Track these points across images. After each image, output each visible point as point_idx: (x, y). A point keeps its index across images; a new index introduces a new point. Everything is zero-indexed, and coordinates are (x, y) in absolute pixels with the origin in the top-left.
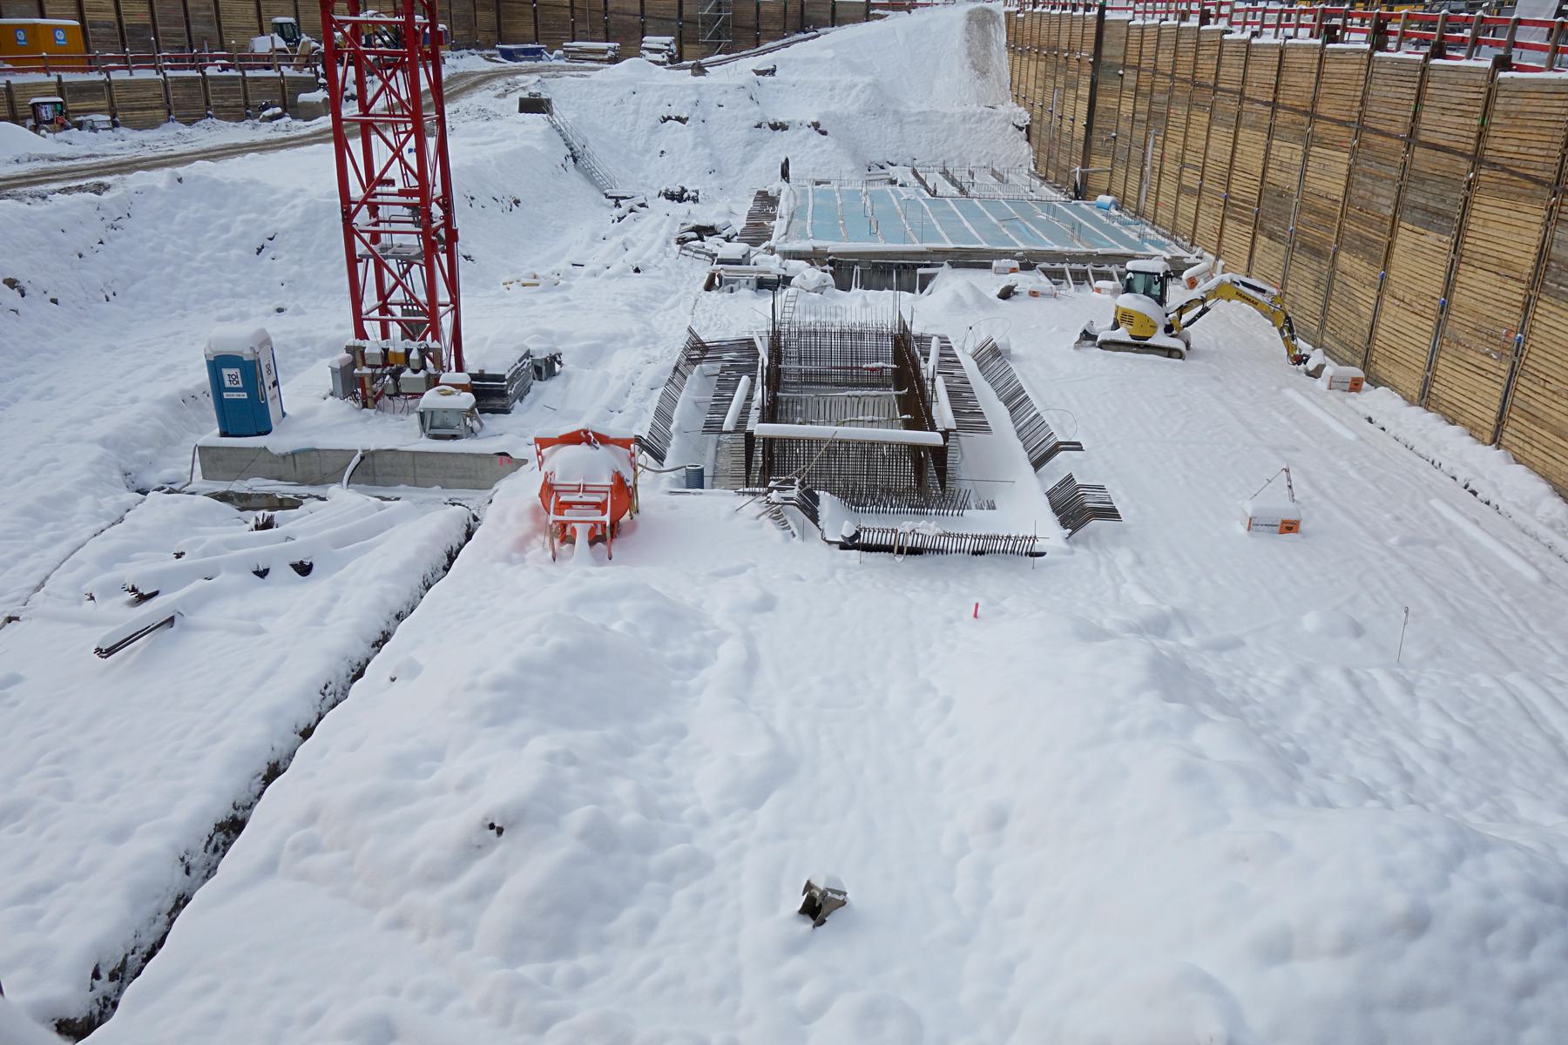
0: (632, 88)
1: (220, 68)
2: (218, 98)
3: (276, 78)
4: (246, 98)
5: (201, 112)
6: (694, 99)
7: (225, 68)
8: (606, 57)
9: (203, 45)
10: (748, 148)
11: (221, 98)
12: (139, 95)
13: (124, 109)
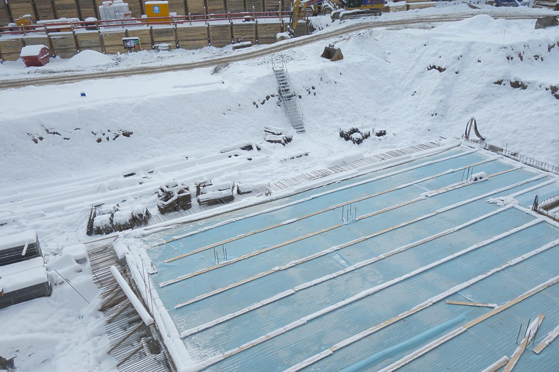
0: (425, 42)
1: (244, 20)
2: (239, 34)
3: (279, 24)
4: (256, 34)
5: (228, 41)
6: (458, 54)
7: (247, 20)
8: (555, 4)
9: (290, 4)
10: (478, 100)
11: (241, 34)
12: (192, 34)
13: (182, 41)
